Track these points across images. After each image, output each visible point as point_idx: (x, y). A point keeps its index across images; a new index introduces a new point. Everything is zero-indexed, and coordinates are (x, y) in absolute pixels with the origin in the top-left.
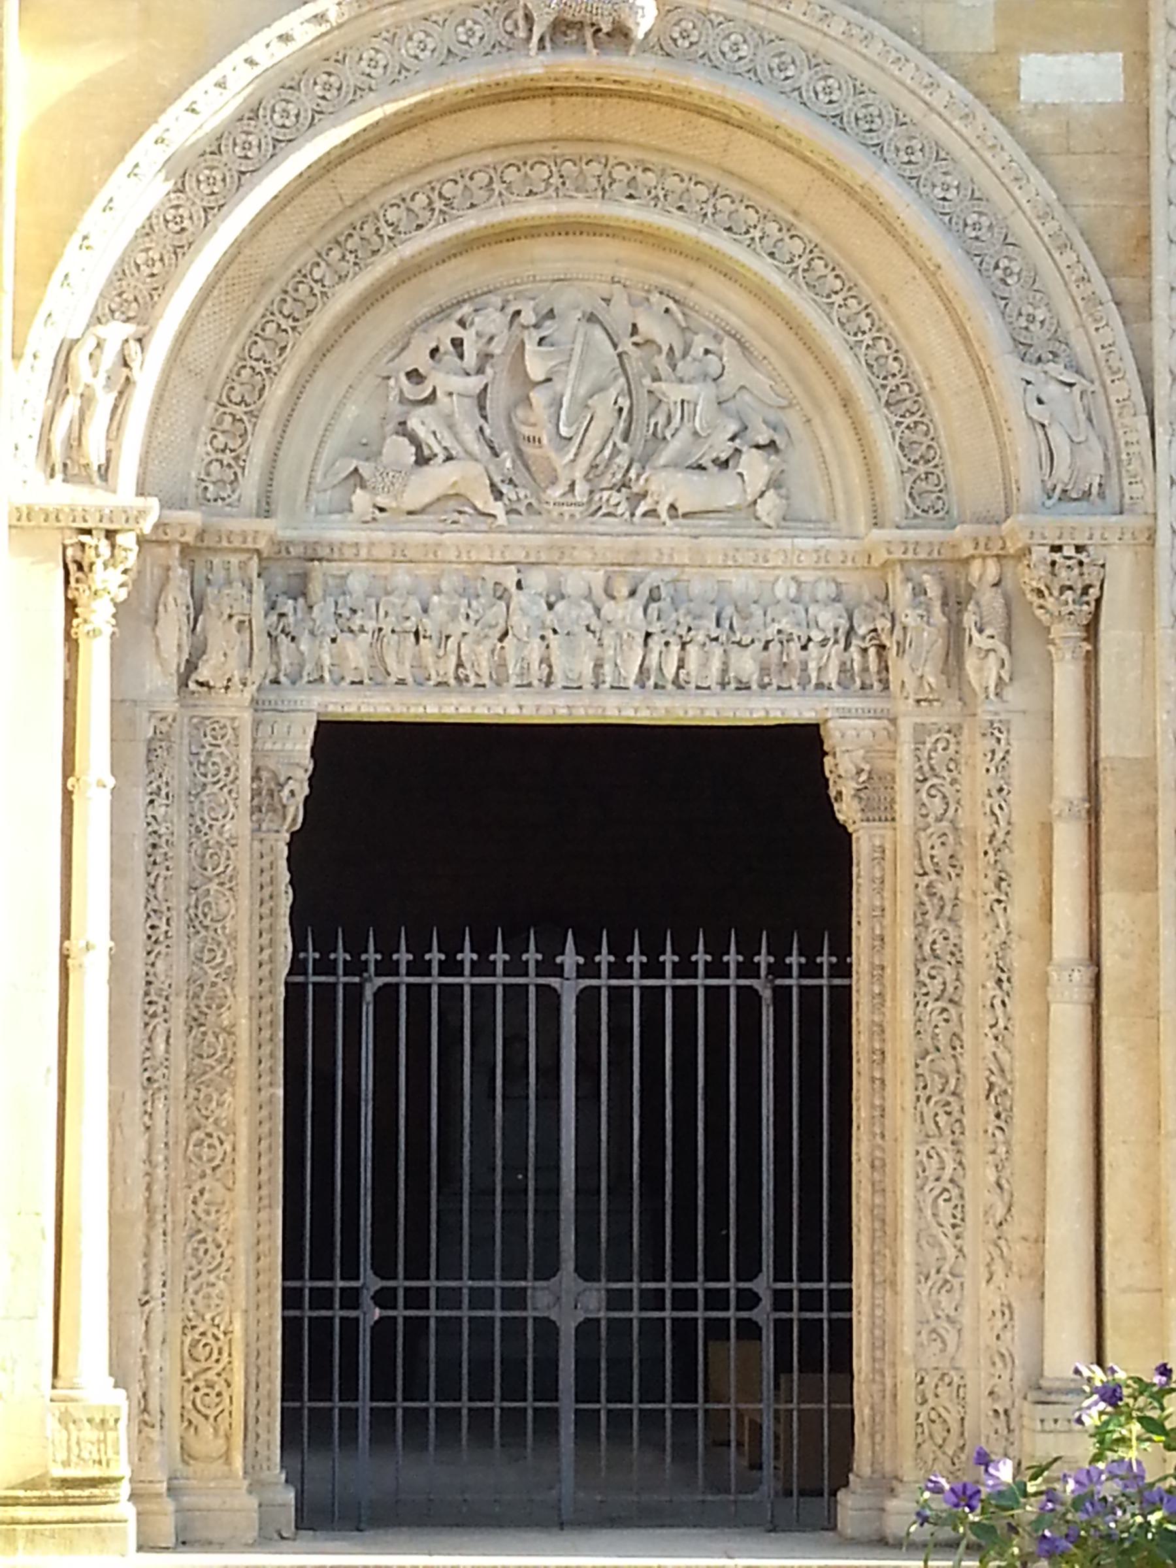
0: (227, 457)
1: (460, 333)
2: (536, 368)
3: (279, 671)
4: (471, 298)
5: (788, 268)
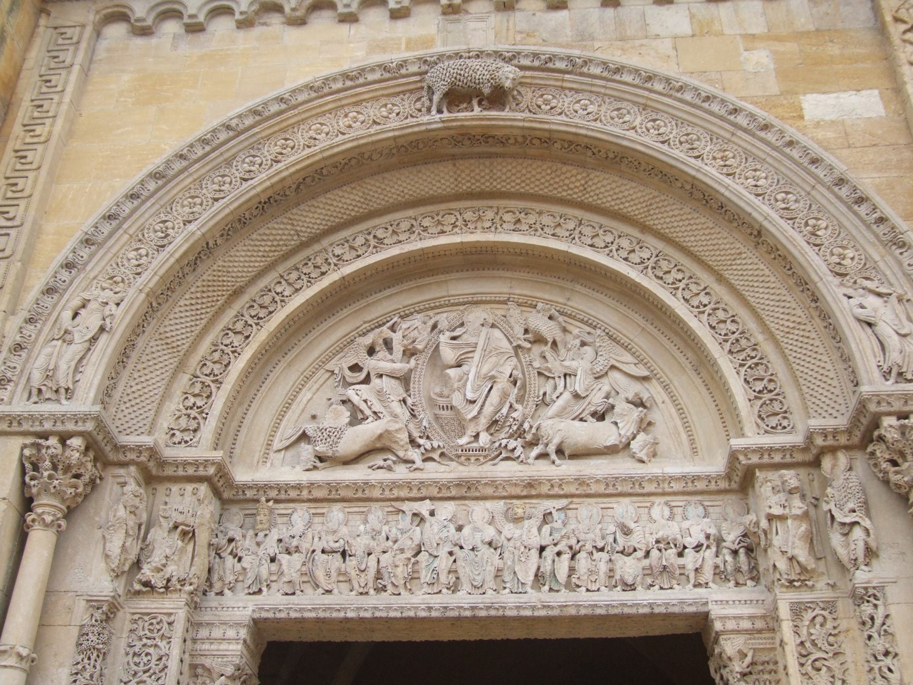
2: (448, 354)
5: (641, 267)
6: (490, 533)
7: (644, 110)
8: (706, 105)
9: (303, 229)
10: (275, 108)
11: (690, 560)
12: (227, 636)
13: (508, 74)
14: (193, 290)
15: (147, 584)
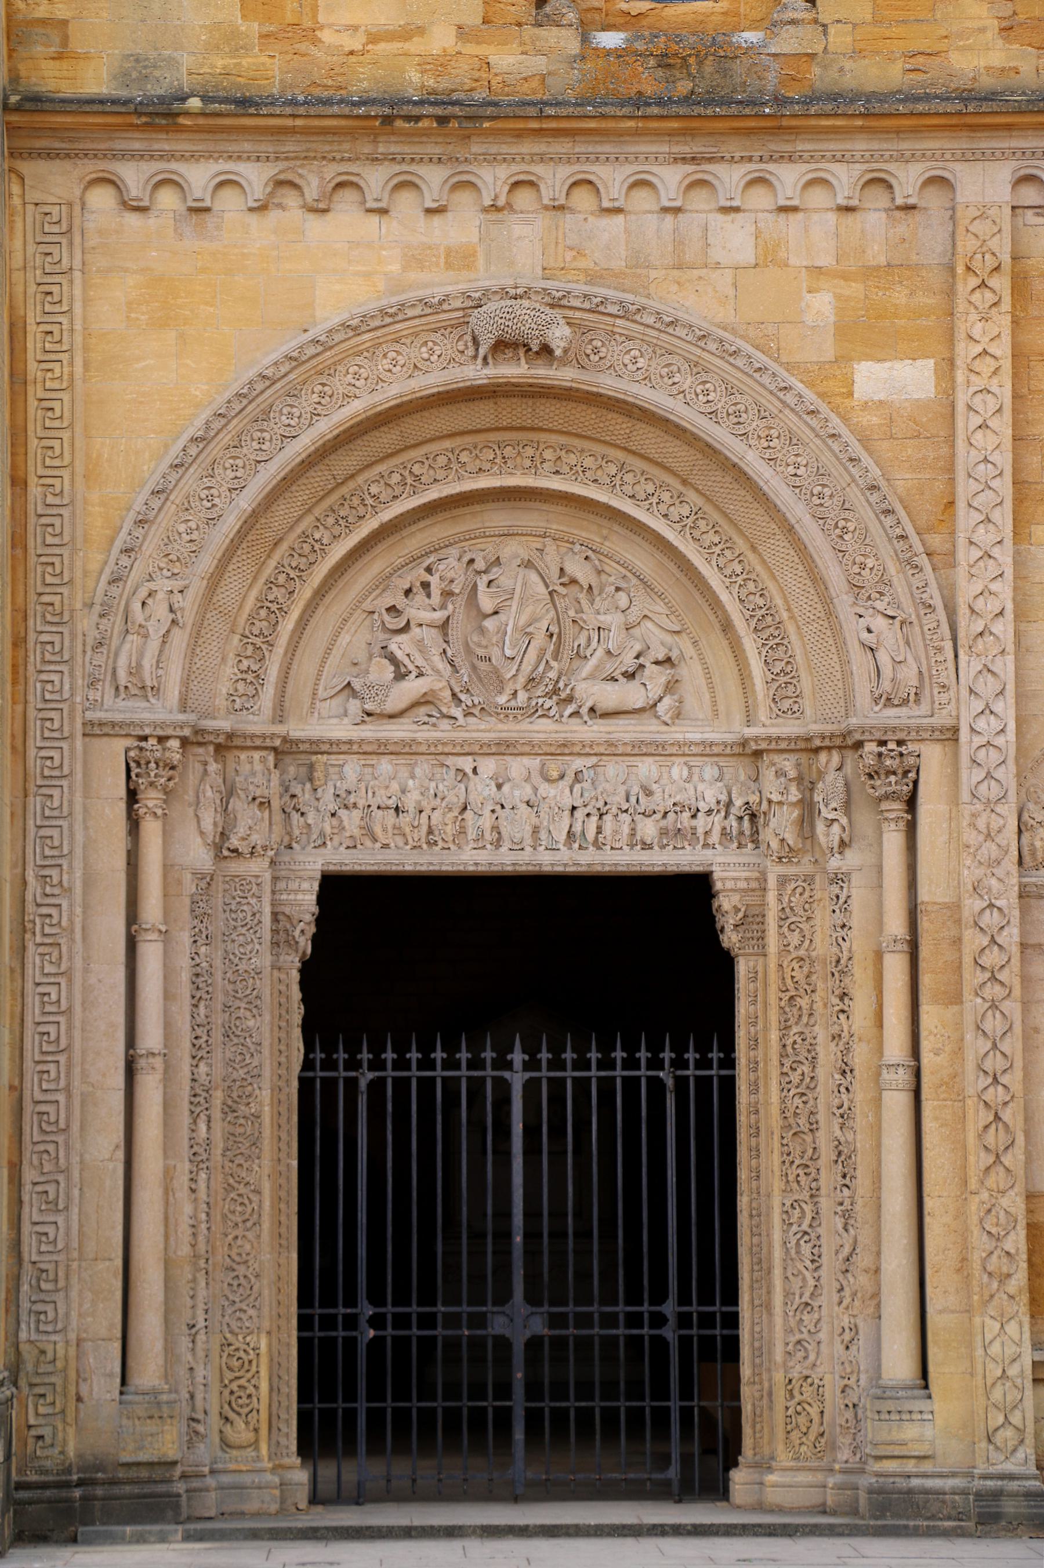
1: (428, 578)
2: (486, 603)
3: (291, 839)
4: (436, 550)
8: (757, 375)
10: (311, 351)
11: (701, 822)
13: (559, 335)
14: (239, 552)
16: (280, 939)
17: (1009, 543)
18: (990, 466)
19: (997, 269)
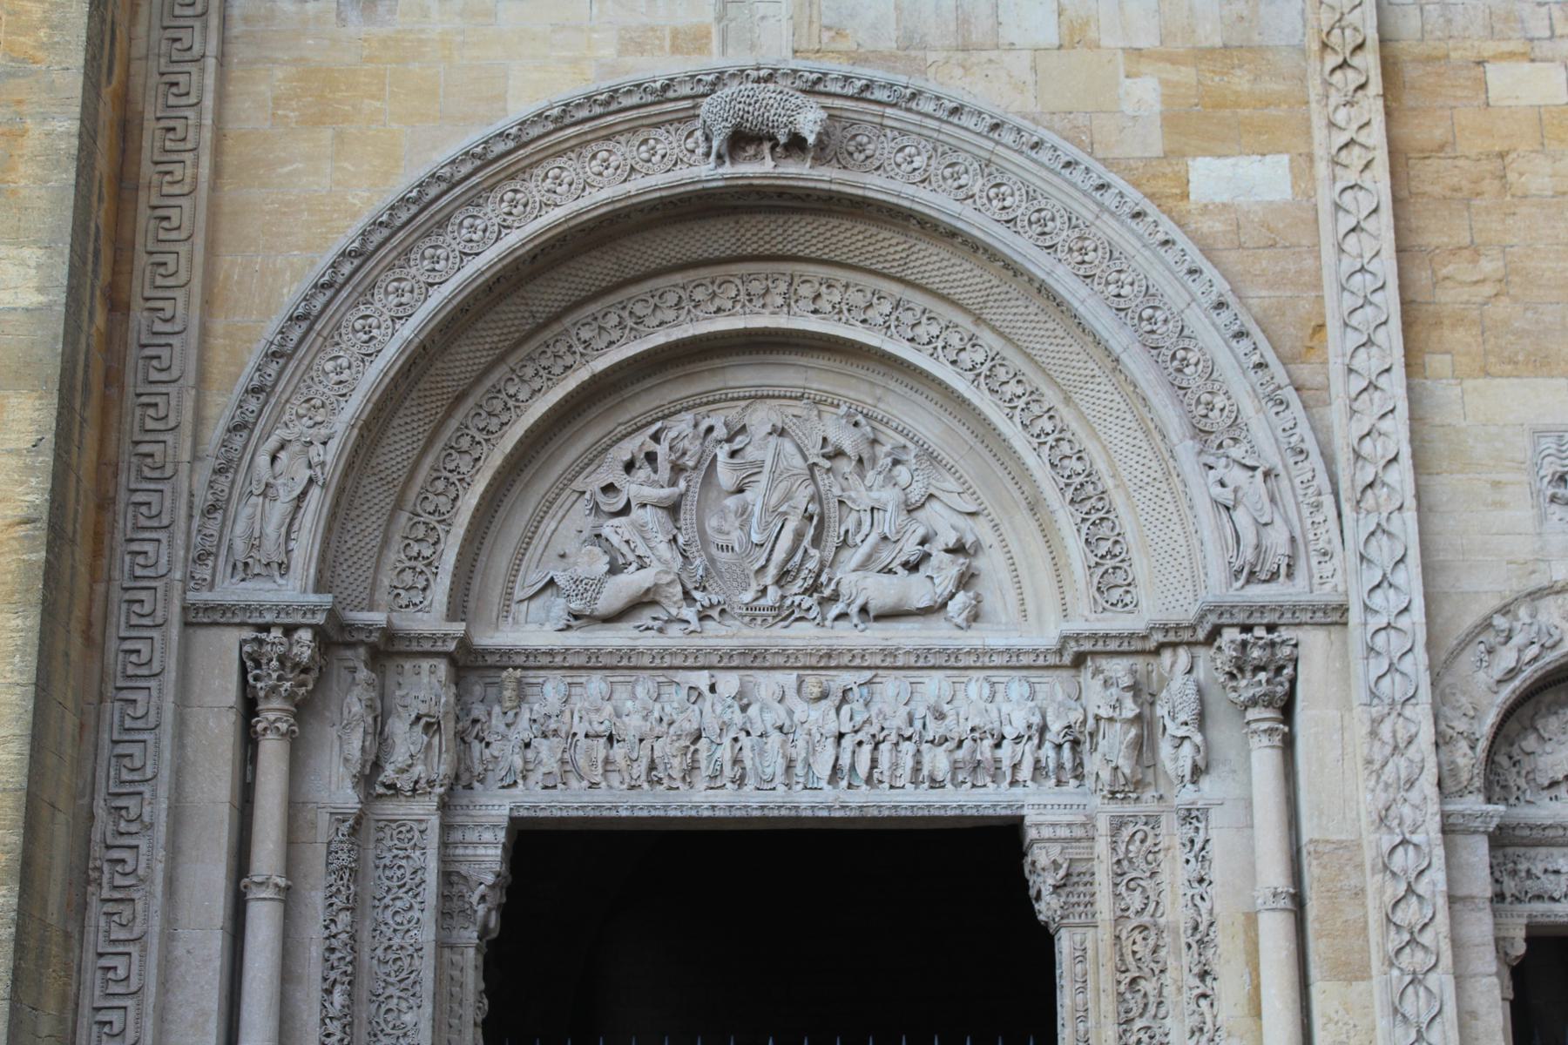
0: (420, 566)
5: (971, 375)
6: (778, 715)
7: (987, 166)
8: (1066, 172)
9: (541, 309)
10: (500, 148)
11: (1006, 752)
12: (483, 840)
13: (809, 121)
14: (407, 404)
15: (392, 786)
16: (449, 908)
17: (1399, 372)
18: (1368, 276)
19: (1360, 47)
